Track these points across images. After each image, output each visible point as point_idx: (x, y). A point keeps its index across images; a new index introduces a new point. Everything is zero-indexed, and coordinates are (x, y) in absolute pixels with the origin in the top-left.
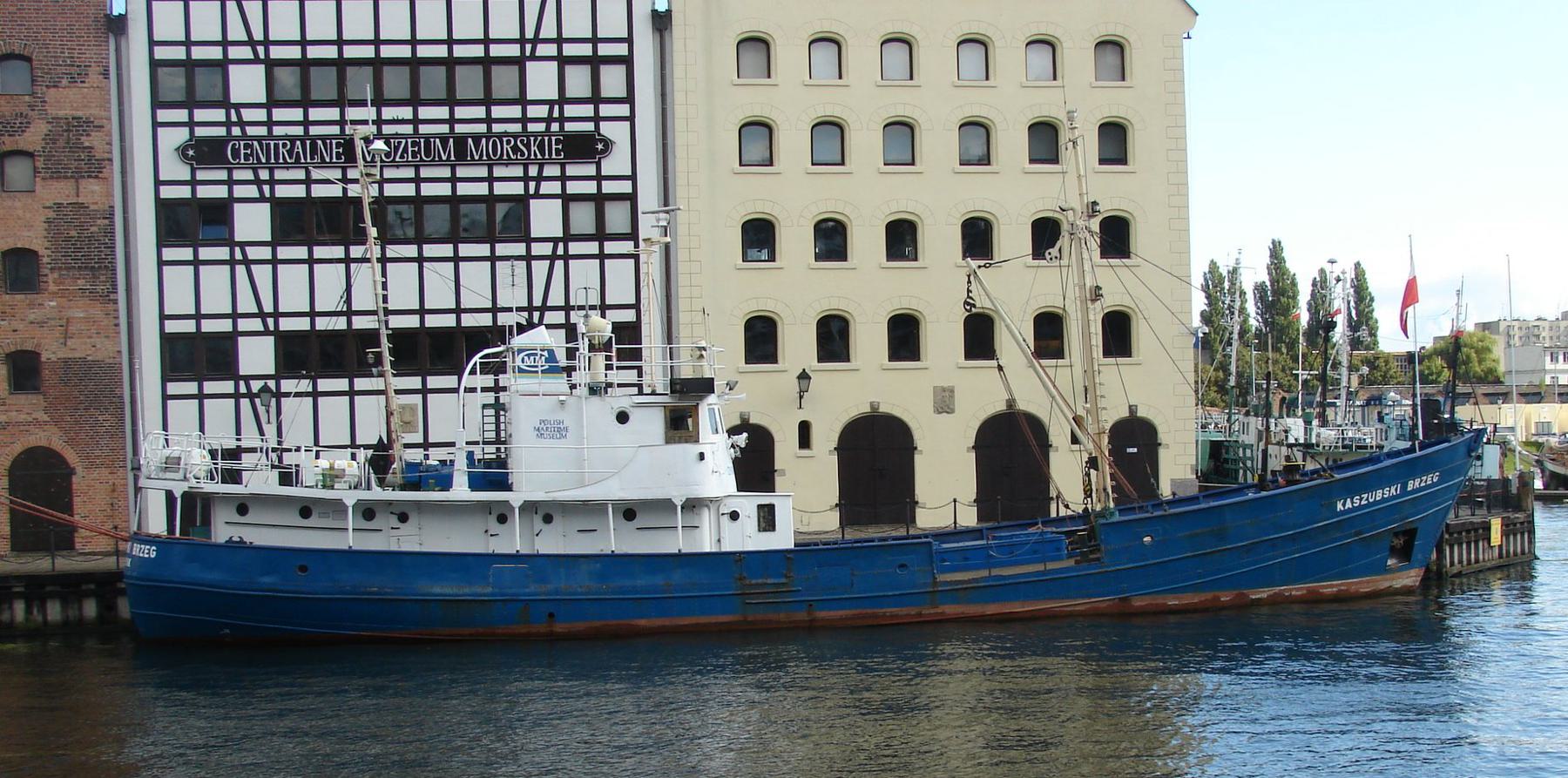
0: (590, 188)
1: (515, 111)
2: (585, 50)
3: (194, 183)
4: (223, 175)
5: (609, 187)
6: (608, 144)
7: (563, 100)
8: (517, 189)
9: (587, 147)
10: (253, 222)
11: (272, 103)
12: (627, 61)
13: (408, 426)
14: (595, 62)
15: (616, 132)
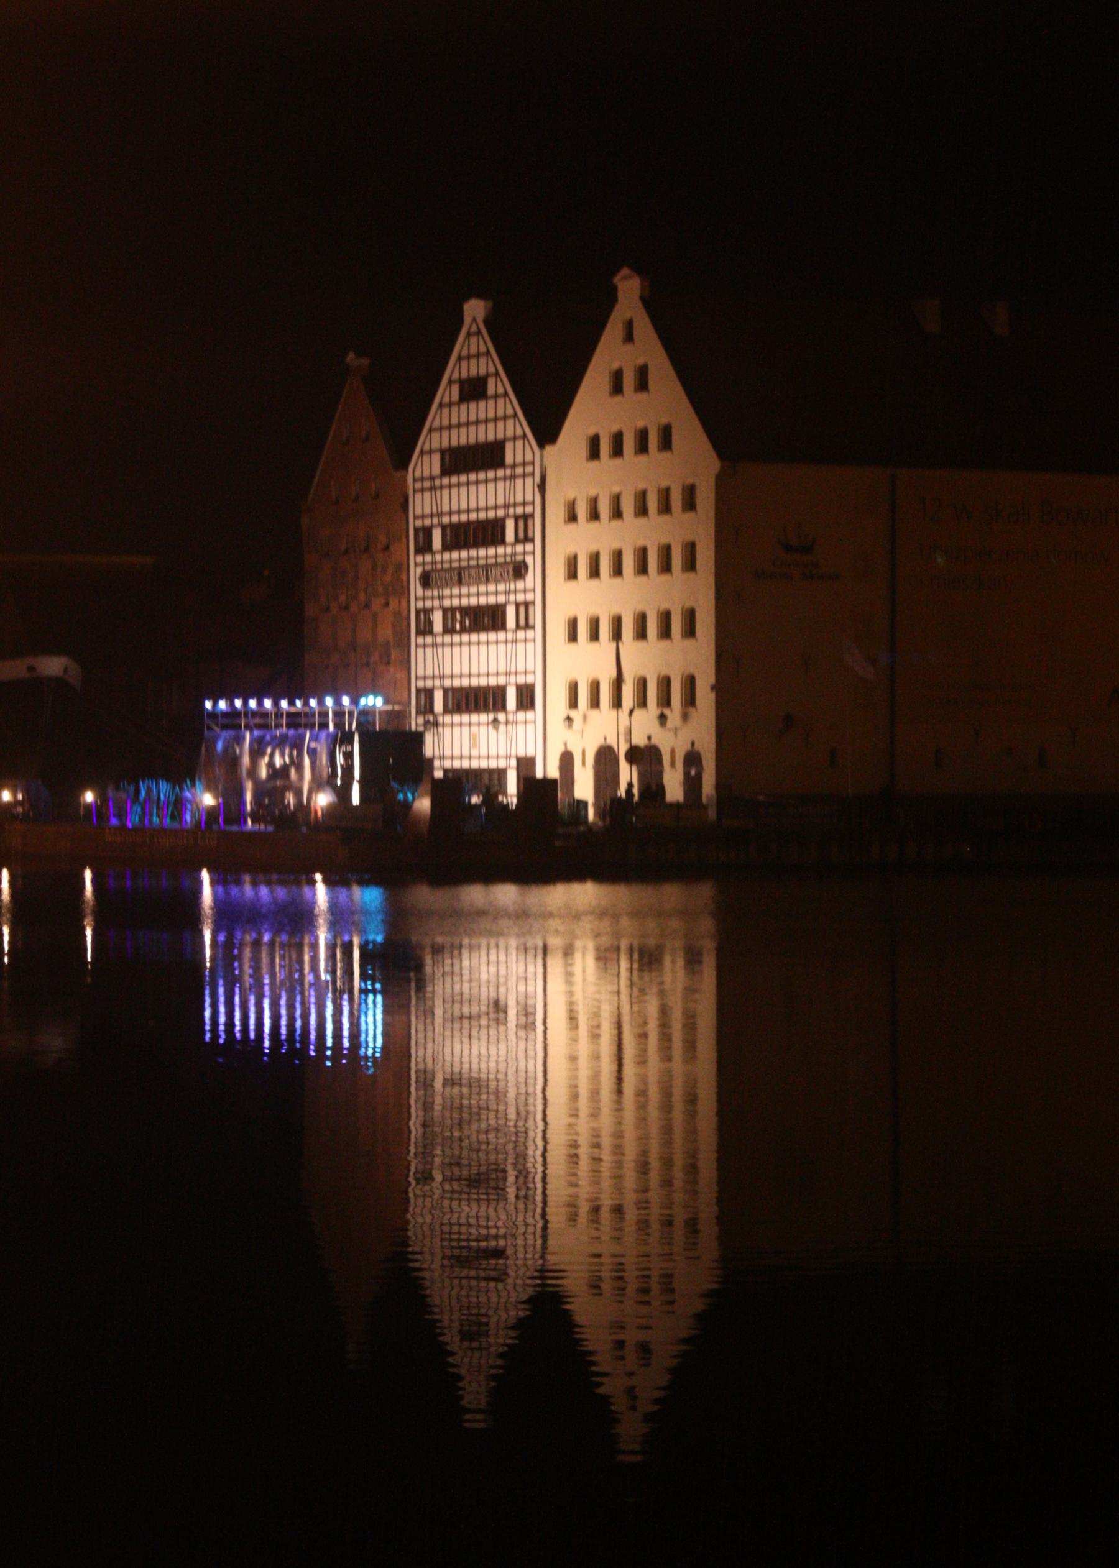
0: (520, 598)
1: (501, 550)
2: (520, 510)
3: (424, 599)
4: (429, 593)
5: (530, 597)
6: (526, 567)
7: (517, 540)
8: (501, 599)
9: (519, 570)
10: (437, 619)
11: (446, 547)
12: (532, 515)
13: (475, 746)
14: (527, 518)
15: (529, 560)
